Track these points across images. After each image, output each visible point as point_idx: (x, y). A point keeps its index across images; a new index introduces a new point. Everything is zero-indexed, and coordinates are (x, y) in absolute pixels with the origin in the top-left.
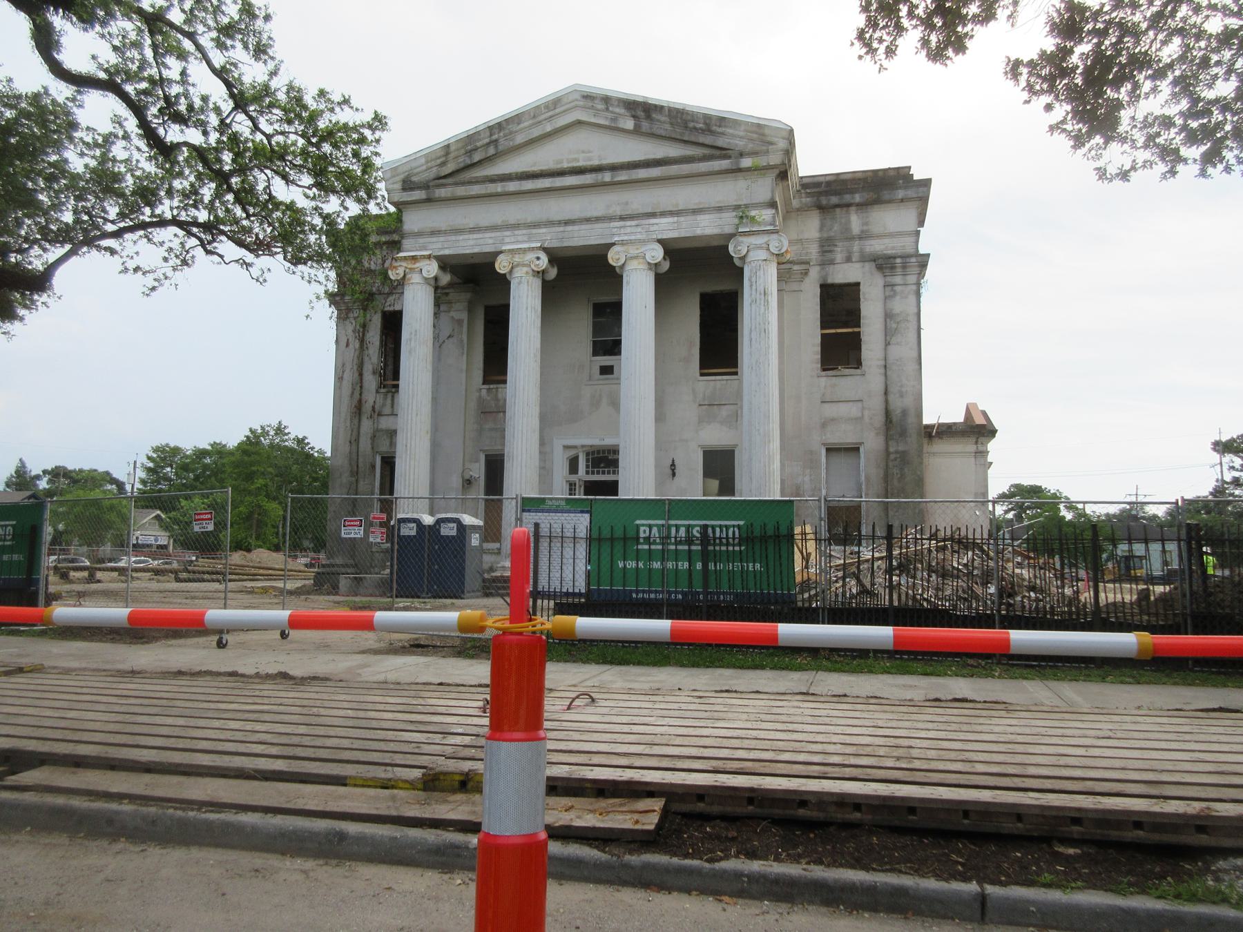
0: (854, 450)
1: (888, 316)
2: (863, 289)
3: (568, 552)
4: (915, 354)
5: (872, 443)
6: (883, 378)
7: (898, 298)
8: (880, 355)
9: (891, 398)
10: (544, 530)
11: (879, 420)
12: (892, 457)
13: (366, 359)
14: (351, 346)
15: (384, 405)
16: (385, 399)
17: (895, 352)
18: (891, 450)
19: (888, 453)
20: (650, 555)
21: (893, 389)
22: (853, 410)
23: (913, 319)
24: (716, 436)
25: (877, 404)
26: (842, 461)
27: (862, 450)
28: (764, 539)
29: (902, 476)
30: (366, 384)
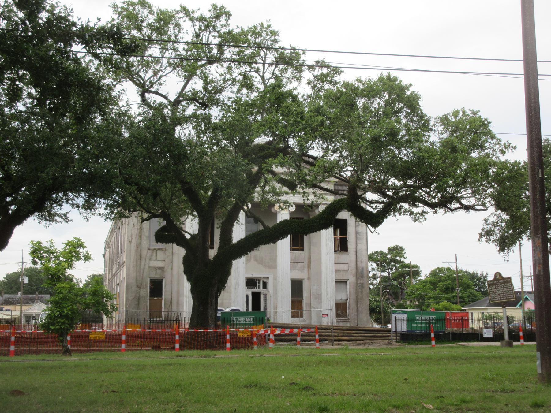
0: (345, 282)
1: (357, 233)
2: (348, 222)
3: (402, 322)
4: (366, 248)
5: (351, 279)
6: (355, 256)
7: (360, 227)
8: (354, 247)
9: (358, 263)
10: (397, 318)
11: (354, 271)
12: (359, 285)
13: (143, 234)
14: (136, 227)
15: (152, 255)
16: (153, 252)
17: (359, 246)
18: (358, 282)
19: (357, 284)
20: (419, 323)
21: (359, 260)
22: (345, 267)
23: (365, 235)
24: (298, 276)
25: (353, 265)
26: (342, 285)
27: (348, 282)
28: (440, 320)
29: (362, 292)
30: (143, 246)
